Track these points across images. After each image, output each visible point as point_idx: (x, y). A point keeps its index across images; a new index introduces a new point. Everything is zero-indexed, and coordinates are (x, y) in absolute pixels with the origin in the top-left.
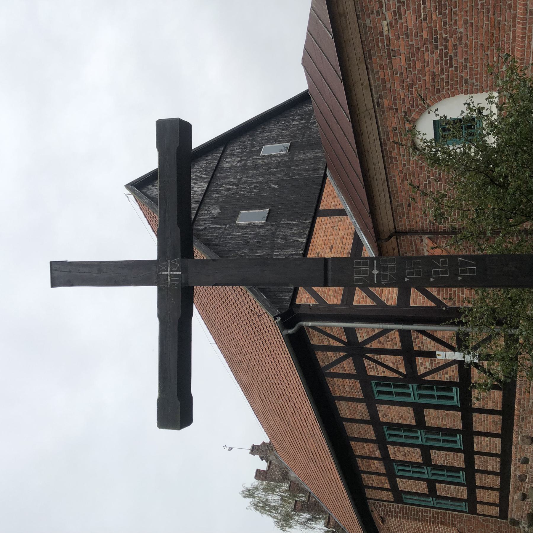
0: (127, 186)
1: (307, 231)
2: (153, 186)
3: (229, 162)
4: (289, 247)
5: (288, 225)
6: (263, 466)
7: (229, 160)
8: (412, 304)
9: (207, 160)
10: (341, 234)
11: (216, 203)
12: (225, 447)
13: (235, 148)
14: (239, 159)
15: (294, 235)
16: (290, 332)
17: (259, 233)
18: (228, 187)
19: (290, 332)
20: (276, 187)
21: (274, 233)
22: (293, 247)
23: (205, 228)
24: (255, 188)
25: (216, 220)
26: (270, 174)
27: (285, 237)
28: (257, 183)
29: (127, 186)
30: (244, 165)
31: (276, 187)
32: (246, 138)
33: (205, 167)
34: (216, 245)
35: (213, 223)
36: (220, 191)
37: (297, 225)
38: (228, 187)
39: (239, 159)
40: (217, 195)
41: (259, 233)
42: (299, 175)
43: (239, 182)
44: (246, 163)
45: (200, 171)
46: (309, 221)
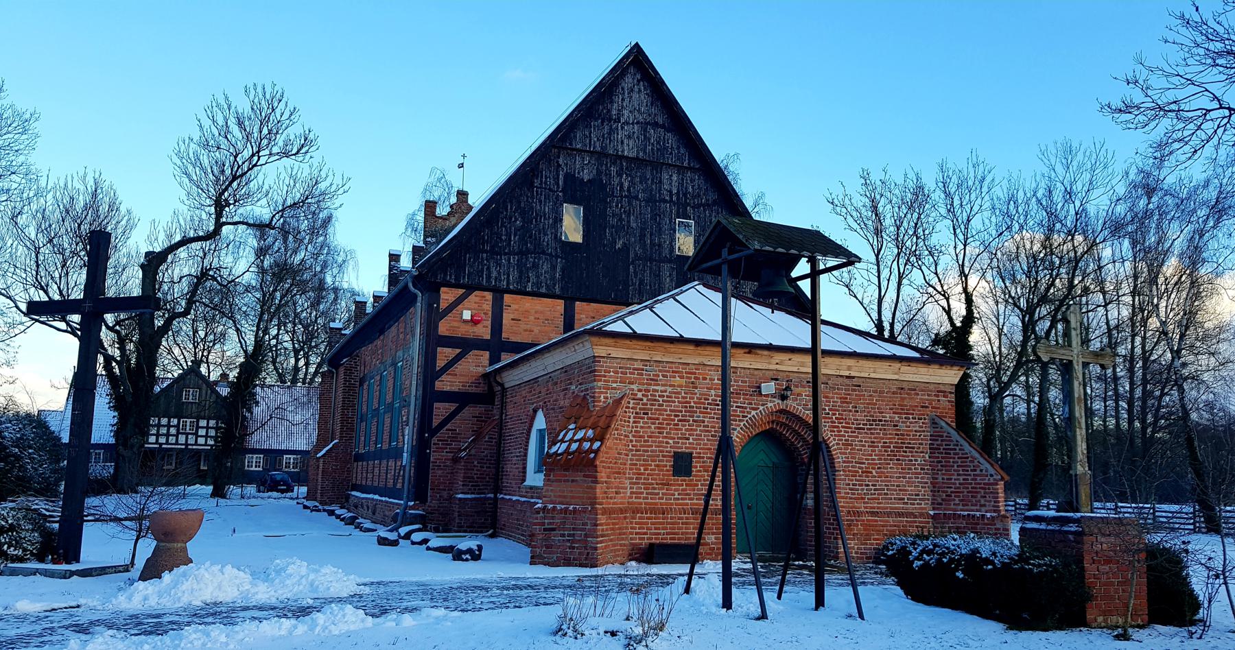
0: (637, 44)
1: (543, 290)
2: (639, 81)
3: (671, 181)
4: (521, 272)
5: (554, 268)
6: (442, 210)
7: (675, 178)
8: (436, 405)
9: (678, 148)
10: (536, 330)
11: (599, 173)
12: (464, 156)
13: (695, 183)
14: (675, 191)
15: (537, 277)
16: (410, 285)
17: (545, 234)
18: (626, 185)
19: (410, 285)
20: (618, 246)
21: (543, 253)
22: (520, 277)
23: (559, 166)
24: (621, 220)
25: (570, 177)
26: (642, 236)
27: (535, 266)
28: (629, 222)
29: (637, 44)
30: (665, 201)
31: (618, 246)
32: (712, 196)
33: (666, 148)
34: (532, 185)
35: (566, 176)
36: (620, 175)
37: (553, 278)
38: (626, 185)
39: (675, 191)
40: (613, 173)
41: (545, 234)
42: (635, 272)
43: (632, 197)
44: (665, 201)
45: (658, 143)
46: (558, 291)
